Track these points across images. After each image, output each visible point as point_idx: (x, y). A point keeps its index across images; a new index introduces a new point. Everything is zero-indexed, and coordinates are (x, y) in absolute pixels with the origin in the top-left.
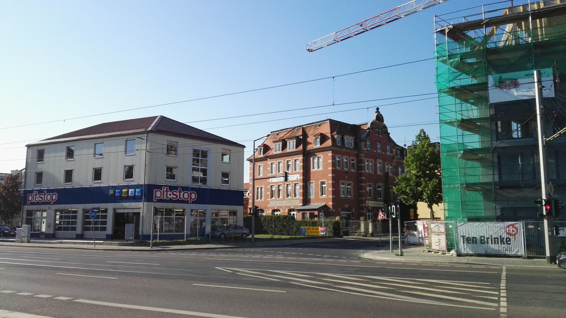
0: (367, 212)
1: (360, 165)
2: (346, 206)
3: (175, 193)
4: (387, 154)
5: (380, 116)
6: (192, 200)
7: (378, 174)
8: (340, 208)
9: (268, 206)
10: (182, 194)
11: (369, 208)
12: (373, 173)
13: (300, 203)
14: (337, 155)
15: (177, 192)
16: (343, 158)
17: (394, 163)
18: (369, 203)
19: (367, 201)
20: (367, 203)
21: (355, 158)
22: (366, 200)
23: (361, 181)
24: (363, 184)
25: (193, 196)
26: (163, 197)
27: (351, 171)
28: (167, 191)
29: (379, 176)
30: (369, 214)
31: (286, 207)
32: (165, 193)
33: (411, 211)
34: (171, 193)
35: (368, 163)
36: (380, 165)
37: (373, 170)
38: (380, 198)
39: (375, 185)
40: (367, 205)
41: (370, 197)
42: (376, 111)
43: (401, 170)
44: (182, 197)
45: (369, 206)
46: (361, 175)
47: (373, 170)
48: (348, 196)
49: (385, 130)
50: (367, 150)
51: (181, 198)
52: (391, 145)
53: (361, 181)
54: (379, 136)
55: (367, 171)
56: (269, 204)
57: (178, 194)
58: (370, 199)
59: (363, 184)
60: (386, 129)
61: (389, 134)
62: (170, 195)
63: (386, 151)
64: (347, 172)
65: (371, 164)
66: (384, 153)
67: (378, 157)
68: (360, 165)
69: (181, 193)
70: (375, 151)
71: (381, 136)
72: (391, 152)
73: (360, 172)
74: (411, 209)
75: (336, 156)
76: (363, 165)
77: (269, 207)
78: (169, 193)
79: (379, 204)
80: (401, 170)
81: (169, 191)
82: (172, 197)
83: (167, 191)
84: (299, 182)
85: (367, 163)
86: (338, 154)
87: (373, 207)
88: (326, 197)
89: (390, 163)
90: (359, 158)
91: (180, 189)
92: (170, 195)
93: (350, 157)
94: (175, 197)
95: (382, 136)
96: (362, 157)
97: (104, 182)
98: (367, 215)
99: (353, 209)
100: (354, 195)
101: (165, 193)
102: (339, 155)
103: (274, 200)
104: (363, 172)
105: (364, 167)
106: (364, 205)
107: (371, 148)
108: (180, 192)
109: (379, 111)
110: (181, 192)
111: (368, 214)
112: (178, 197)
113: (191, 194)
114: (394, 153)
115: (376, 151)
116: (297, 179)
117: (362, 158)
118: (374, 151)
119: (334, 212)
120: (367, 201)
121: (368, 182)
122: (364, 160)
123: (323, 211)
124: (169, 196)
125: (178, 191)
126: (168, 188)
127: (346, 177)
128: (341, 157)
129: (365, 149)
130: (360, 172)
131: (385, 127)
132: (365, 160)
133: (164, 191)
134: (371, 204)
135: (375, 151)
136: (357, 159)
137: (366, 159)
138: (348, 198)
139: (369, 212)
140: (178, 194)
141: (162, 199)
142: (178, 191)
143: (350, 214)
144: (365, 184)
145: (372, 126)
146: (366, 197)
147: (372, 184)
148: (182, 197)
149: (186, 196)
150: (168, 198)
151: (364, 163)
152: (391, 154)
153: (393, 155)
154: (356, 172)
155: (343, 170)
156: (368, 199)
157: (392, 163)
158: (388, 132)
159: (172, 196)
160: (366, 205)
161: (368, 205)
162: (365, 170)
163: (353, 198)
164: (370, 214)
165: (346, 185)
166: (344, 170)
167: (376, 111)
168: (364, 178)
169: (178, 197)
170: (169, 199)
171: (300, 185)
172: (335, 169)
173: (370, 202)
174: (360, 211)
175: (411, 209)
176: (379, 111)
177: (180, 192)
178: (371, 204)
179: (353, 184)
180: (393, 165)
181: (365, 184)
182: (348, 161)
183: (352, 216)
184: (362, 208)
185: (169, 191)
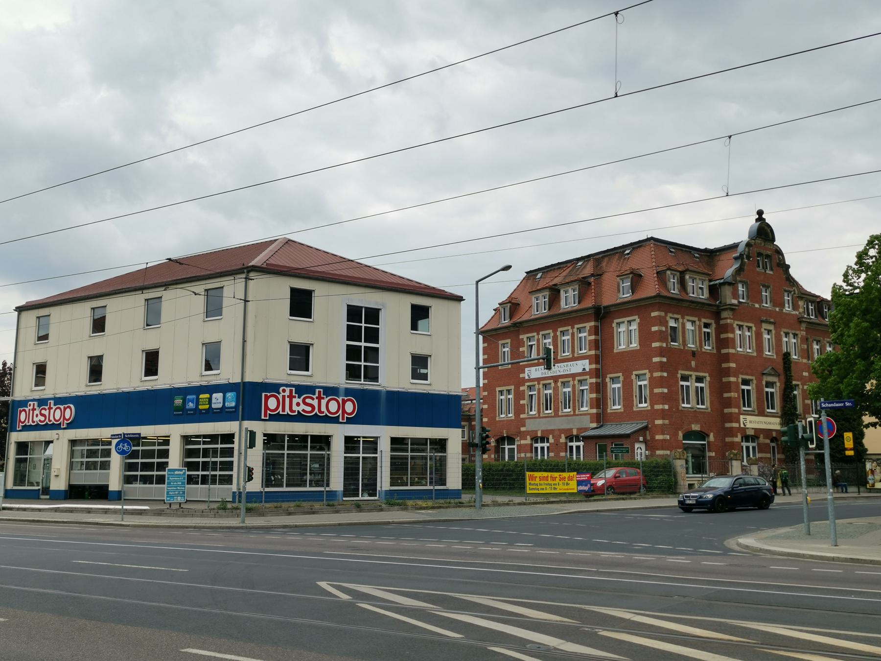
0: (742, 441)
1: (723, 336)
2: (696, 427)
3: (308, 401)
4: (784, 311)
5: (766, 228)
6: (346, 415)
7: (764, 356)
8: (680, 432)
9: (523, 429)
11: (747, 430)
12: (755, 354)
13: (591, 422)
14: (670, 315)
15: (313, 399)
16: (685, 321)
18: (748, 421)
19: (742, 417)
20: (742, 420)
21: (713, 322)
22: (740, 414)
23: (727, 372)
24: (733, 379)
25: (349, 407)
26: (284, 410)
27: (703, 350)
28: (291, 397)
29: (769, 360)
30: (748, 444)
31: (561, 431)
32: (287, 400)
33: (845, 437)
34: (300, 400)
35: (742, 332)
36: (769, 337)
37: (755, 348)
38: (772, 409)
39: (759, 381)
40: (742, 426)
41: (749, 406)
42: (757, 216)
43: (818, 347)
44: (323, 409)
45: (748, 428)
46: (727, 358)
47: (753, 347)
48: (698, 404)
49: (779, 258)
50: (739, 302)
51: (323, 412)
52: (794, 291)
53: (727, 372)
54: (765, 271)
55: (739, 349)
56: (524, 426)
57: (315, 403)
58: (750, 413)
59: (733, 379)
60: (781, 257)
61: (788, 267)
62: (298, 404)
63: (782, 305)
64: (694, 354)
65: (748, 334)
66: (777, 309)
67: (765, 318)
68: (723, 336)
69: (322, 400)
70: (757, 306)
71: (768, 272)
72: (795, 307)
73: (724, 351)
74: (845, 433)
75: (668, 318)
76: (731, 335)
77: (524, 432)
78: (295, 401)
79: (770, 423)
80: (818, 347)
81: (297, 395)
82: (303, 410)
83: (291, 397)
84: (588, 377)
85: (738, 332)
86: (673, 313)
87: (756, 430)
88: (649, 408)
89: (794, 332)
90: (722, 322)
91: (320, 392)
92: (298, 404)
93: (700, 320)
94: (309, 409)
95: (771, 273)
96: (726, 318)
97: (163, 380)
98: (742, 447)
99: (712, 435)
100: (712, 403)
101: (287, 400)
102: (676, 316)
103: (535, 418)
104: (732, 351)
105: (733, 340)
106: (735, 425)
107: (748, 297)
108: (320, 399)
109: (764, 216)
110: (323, 398)
111: (744, 444)
112: (316, 410)
113: (344, 402)
114: (801, 310)
115: (760, 306)
116: (584, 369)
117: (729, 321)
118: (754, 305)
120: (742, 417)
121: (742, 374)
122: (732, 325)
123: (641, 439)
124: (295, 408)
125: (314, 397)
127: (693, 363)
128: (681, 320)
129: (735, 302)
130: (724, 351)
131: (779, 252)
132: (735, 326)
133: (284, 397)
134: (751, 422)
135: (757, 306)
136: (717, 323)
137: (736, 322)
138: (698, 410)
139: (747, 441)
140: (315, 403)
141: (281, 413)
142: (314, 397)
143: (705, 444)
144: (737, 380)
145: (749, 250)
146: (739, 408)
147: (753, 378)
148: (323, 409)
149: (333, 406)
150: (295, 411)
151: (733, 332)
152: (794, 313)
153: (799, 313)
154: (715, 351)
155: (684, 347)
156: (744, 412)
157: (797, 332)
158: (787, 263)
159: (303, 407)
160: (740, 425)
161: (744, 424)
162: (734, 347)
163: (709, 410)
164: (751, 445)
165: (694, 380)
166: (686, 349)
167: (757, 216)
168: (733, 365)
169: (316, 410)
170: (296, 413)
171: (591, 384)
172: (667, 345)
173: (749, 418)
174: (728, 439)
175: (845, 433)
176: (764, 216)
177: (320, 399)
178: (751, 422)
179: (708, 379)
180: (800, 336)
181: (738, 378)
182: (695, 327)
183: (709, 451)
184: (732, 432)
185: (295, 397)
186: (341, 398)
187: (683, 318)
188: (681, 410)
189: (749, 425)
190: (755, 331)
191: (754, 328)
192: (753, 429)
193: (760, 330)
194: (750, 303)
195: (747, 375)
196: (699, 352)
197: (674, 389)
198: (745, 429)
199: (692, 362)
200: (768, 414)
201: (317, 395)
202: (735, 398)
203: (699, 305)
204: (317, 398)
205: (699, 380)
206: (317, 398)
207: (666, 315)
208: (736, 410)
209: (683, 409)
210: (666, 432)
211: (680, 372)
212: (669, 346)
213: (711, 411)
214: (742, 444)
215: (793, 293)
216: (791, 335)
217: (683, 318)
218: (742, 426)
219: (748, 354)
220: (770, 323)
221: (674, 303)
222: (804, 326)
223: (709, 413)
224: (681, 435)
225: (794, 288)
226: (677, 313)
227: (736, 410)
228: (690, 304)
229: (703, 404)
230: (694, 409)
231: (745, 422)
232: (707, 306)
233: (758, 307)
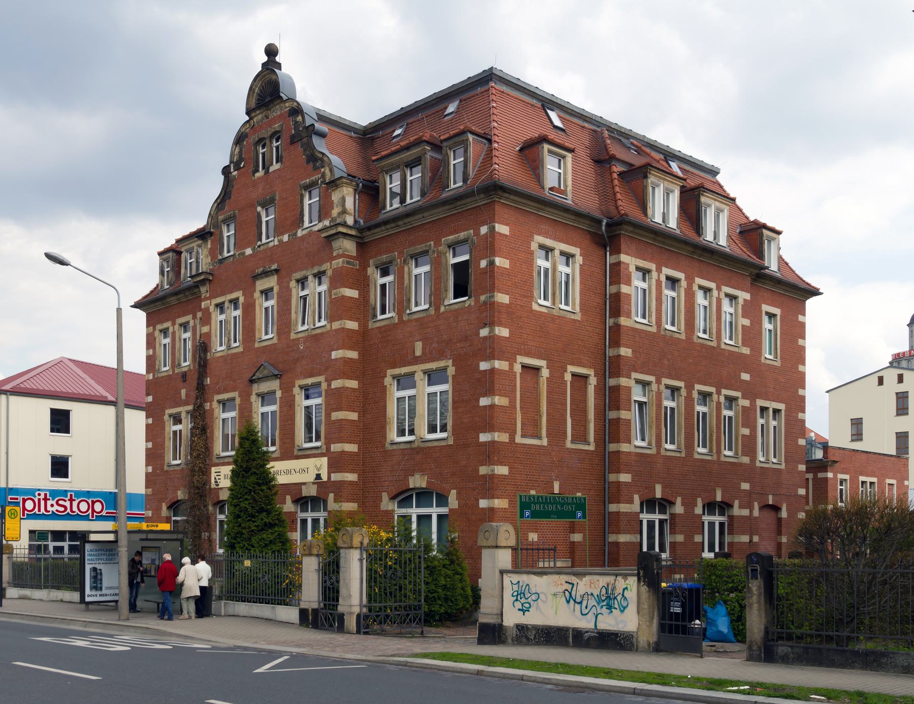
0: (642, 512)
3: (61, 502)
10: (75, 504)
15: (65, 501)
26: (39, 510)
28: (46, 499)
30: (651, 516)
32: (42, 502)
34: (54, 502)
44: (75, 508)
57: (67, 504)
62: (52, 505)
78: (49, 503)
81: (51, 498)
82: (57, 511)
83: (46, 499)
91: (71, 495)
92: (52, 505)
94: (62, 509)
98: (641, 522)
101: (42, 502)
108: (71, 500)
110: (75, 500)
111: (645, 517)
124: (49, 508)
126: (73, 494)
139: (651, 510)
140: (67, 504)
141: (37, 513)
142: (67, 499)
148: (75, 508)
149: (84, 507)
150: (49, 511)
159: (56, 507)
170: (51, 513)
185: (49, 499)
186: (90, 500)
201: (69, 497)
204: (69, 500)
206: (69, 500)
214: (642, 516)
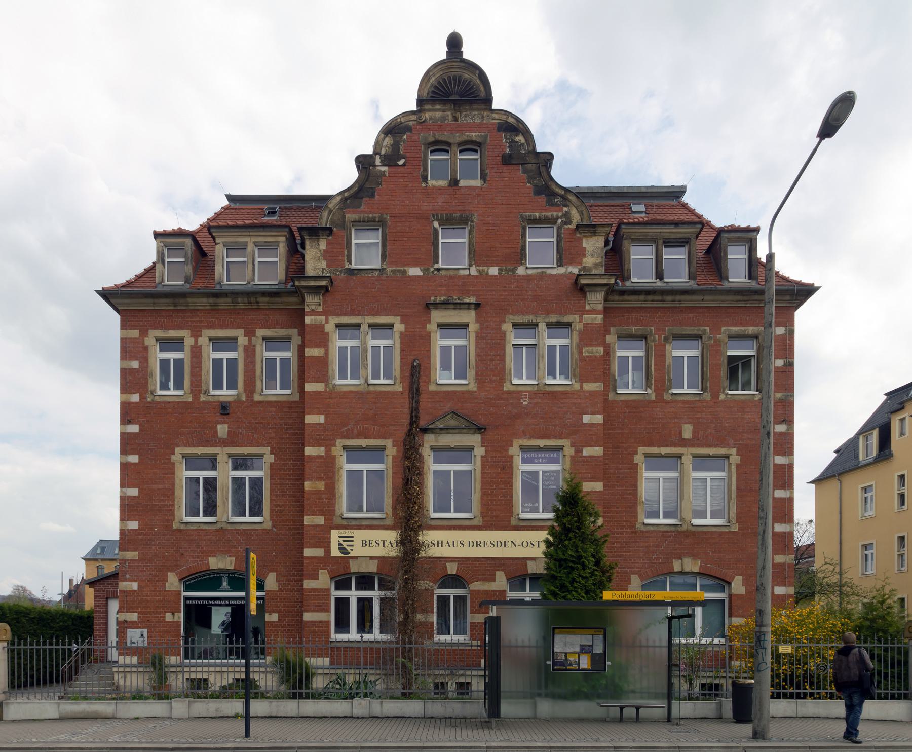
11: (351, 561)
16: (203, 341)
17: (593, 311)
18: (357, 542)
40: (335, 552)
45: (356, 558)
58: (364, 523)
86: (167, 328)
102: (173, 334)
115: (426, 270)
119: (134, 591)
120: (335, 535)
134: (364, 543)
138: (229, 527)
156: (345, 523)
161: (341, 548)
173: (359, 535)
179: (269, 458)
187: (196, 335)
188: (179, 530)
189: (357, 551)
190: (401, 333)
191: (399, 327)
192: (371, 558)
193: (424, 327)
194: (389, 269)
195: (366, 438)
196: (243, 403)
197: (160, 487)
198: (346, 559)
199: (219, 427)
200: (433, 523)
202: (317, 492)
203: (240, 300)
205: (240, 463)
207: (144, 333)
208: (320, 520)
209: (182, 527)
210: (127, 576)
211: (178, 450)
212: (149, 400)
213: (273, 526)
215: (560, 221)
216: (542, 327)
217: (196, 335)
218: (335, 552)
219: (371, 388)
220: (459, 306)
221: (163, 304)
222: (596, 299)
223: (266, 532)
224: (173, 582)
225: (565, 209)
226: (181, 328)
227: (320, 520)
228: (211, 300)
229: (256, 511)
230: (219, 526)
231: (345, 544)
232: (267, 299)
233: (421, 273)
